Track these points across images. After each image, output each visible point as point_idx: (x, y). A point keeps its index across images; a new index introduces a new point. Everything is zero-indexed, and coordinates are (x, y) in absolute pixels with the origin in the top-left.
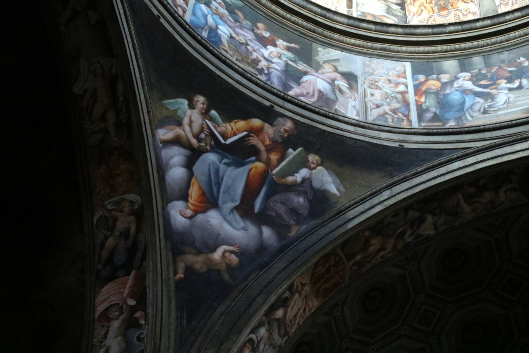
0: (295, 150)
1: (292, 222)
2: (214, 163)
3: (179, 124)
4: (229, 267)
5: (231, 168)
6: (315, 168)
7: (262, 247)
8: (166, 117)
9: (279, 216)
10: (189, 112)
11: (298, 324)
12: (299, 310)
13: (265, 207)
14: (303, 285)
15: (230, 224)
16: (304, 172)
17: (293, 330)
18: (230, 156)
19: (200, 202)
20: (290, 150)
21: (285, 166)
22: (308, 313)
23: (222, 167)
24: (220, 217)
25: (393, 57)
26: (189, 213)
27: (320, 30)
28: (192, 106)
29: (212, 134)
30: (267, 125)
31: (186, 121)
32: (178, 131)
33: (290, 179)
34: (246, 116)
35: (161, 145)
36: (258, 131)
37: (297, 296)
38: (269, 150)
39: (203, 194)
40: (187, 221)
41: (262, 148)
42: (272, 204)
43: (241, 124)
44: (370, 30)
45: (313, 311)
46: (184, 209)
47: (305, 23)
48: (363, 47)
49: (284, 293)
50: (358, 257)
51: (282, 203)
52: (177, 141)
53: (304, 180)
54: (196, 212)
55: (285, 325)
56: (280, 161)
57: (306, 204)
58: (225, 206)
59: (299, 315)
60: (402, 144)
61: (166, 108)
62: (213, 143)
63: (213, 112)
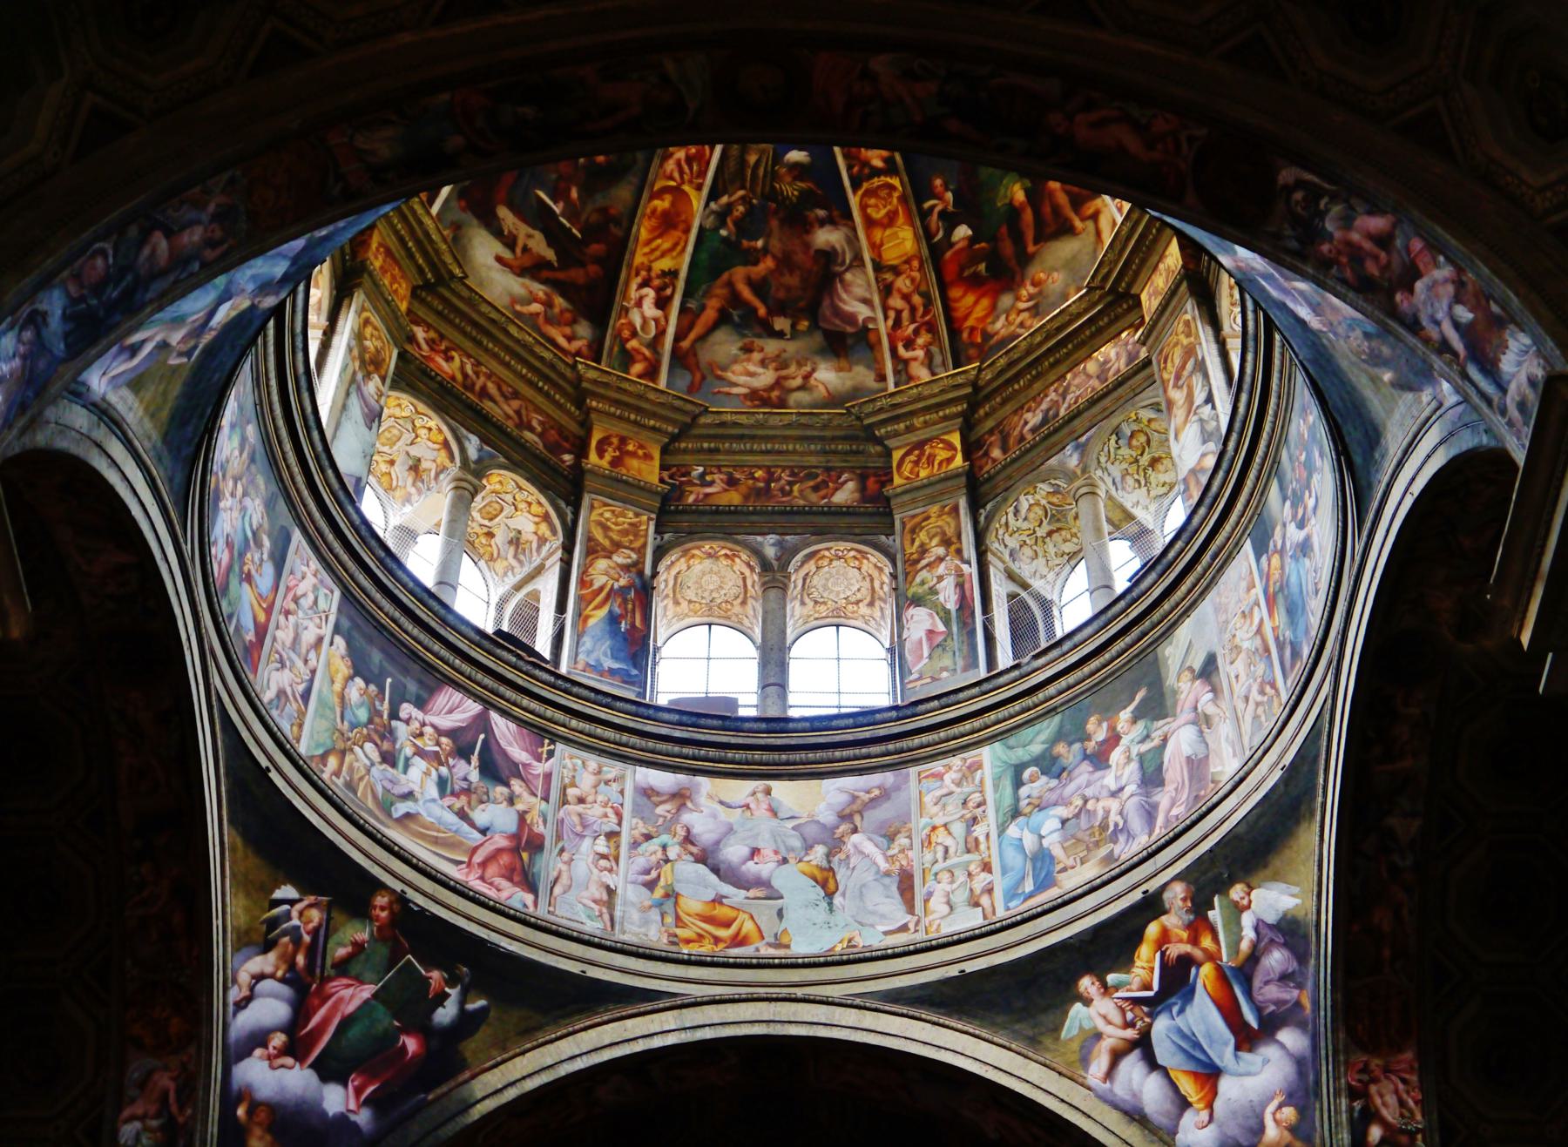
0: (1213, 908)
1: (1296, 993)
2: (1169, 1029)
3: (1098, 1036)
4: (1292, 1129)
5: (1188, 1010)
6: (1250, 902)
7: (1299, 1062)
8: (1082, 1047)
9: (1278, 1003)
10: (1092, 1011)
11: (1416, 1103)
12: (1396, 1092)
13: (1258, 1010)
14: (1365, 1069)
15: (1248, 1074)
16: (1247, 920)
17: (1419, 1117)
18: (1173, 1000)
19: (1202, 1089)
20: (1210, 913)
21: (1226, 937)
22: (1414, 1078)
23: (1179, 1021)
24: (1235, 1079)
25: (1231, 553)
26: (1204, 1115)
27: (1147, 624)
28: (1087, 1002)
29: (1136, 1002)
30: (1164, 918)
31: (1101, 1025)
32: (1106, 1045)
33: (1245, 946)
34: (1137, 938)
35: (1108, 1085)
36: (1165, 937)
37: (1373, 1089)
38: (1194, 941)
39: (1195, 1075)
40: (1212, 1127)
41: (1187, 948)
42: (1260, 998)
43: (1145, 952)
44: (1182, 550)
45: (1416, 1065)
46: (1196, 1119)
47: (1128, 639)
48: (1198, 581)
49: (1351, 1109)
50: (1387, 953)
51: (1267, 983)
52: (1117, 1056)
53: (1256, 929)
54: (1210, 1106)
55: (1402, 1131)
56: (1216, 939)
57: (1286, 953)
58: (1225, 1060)
59: (1405, 1096)
60: (1281, 766)
61: (1071, 1040)
62: (1145, 1009)
63: (1111, 978)
